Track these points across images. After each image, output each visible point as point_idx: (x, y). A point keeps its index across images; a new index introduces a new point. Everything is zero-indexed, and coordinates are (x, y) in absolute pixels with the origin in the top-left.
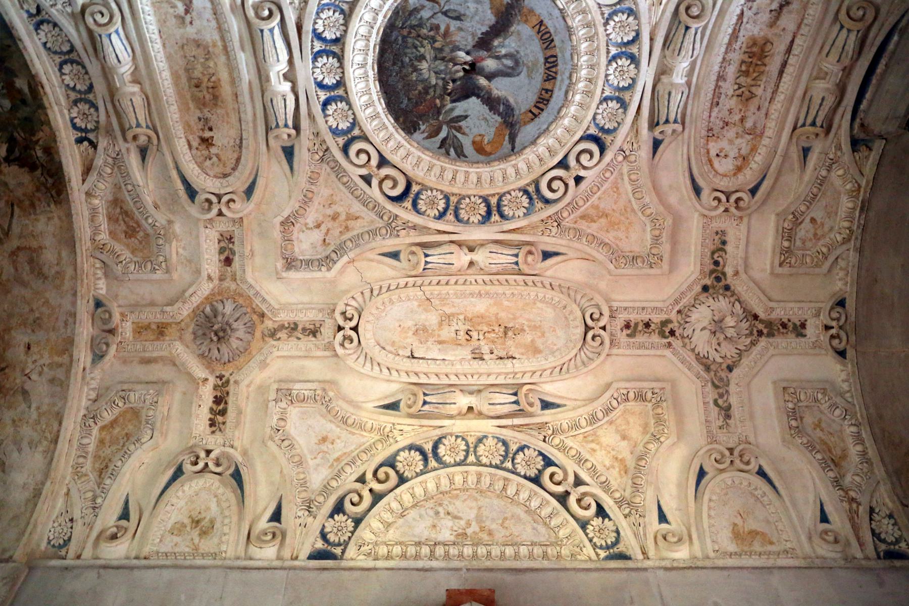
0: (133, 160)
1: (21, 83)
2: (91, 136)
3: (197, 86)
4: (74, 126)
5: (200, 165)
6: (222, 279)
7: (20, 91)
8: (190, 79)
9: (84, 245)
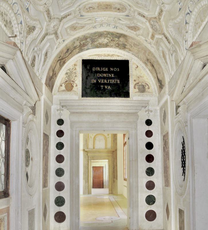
0: (121, 22)
1: (105, 33)
2: (116, 26)
3: (107, 8)
4: (114, 28)
5: (123, 12)
6: (147, 20)
7: (107, 33)
8: (105, 9)
9: (135, 37)
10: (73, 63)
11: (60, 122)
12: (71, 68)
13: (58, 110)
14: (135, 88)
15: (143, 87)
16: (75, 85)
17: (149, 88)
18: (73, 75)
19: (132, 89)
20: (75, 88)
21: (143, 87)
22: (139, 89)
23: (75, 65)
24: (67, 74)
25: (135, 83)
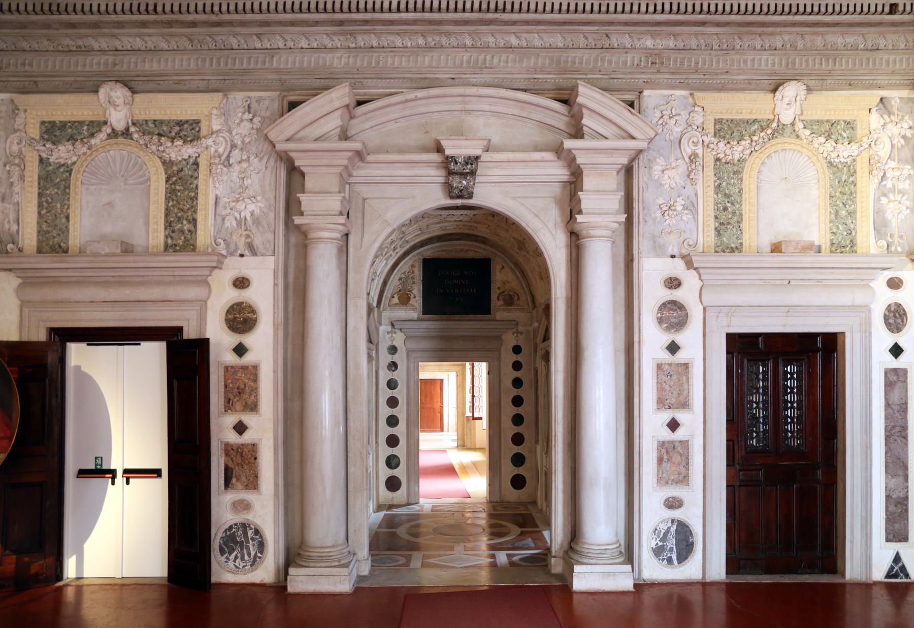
10: (410, 264)
11: (393, 350)
12: (407, 270)
13: (388, 333)
14: (498, 299)
15: (511, 297)
16: (412, 296)
17: (518, 299)
18: (410, 281)
19: (496, 302)
20: (412, 301)
21: (511, 297)
22: (504, 300)
23: (413, 266)
24: (400, 279)
25: (499, 292)
